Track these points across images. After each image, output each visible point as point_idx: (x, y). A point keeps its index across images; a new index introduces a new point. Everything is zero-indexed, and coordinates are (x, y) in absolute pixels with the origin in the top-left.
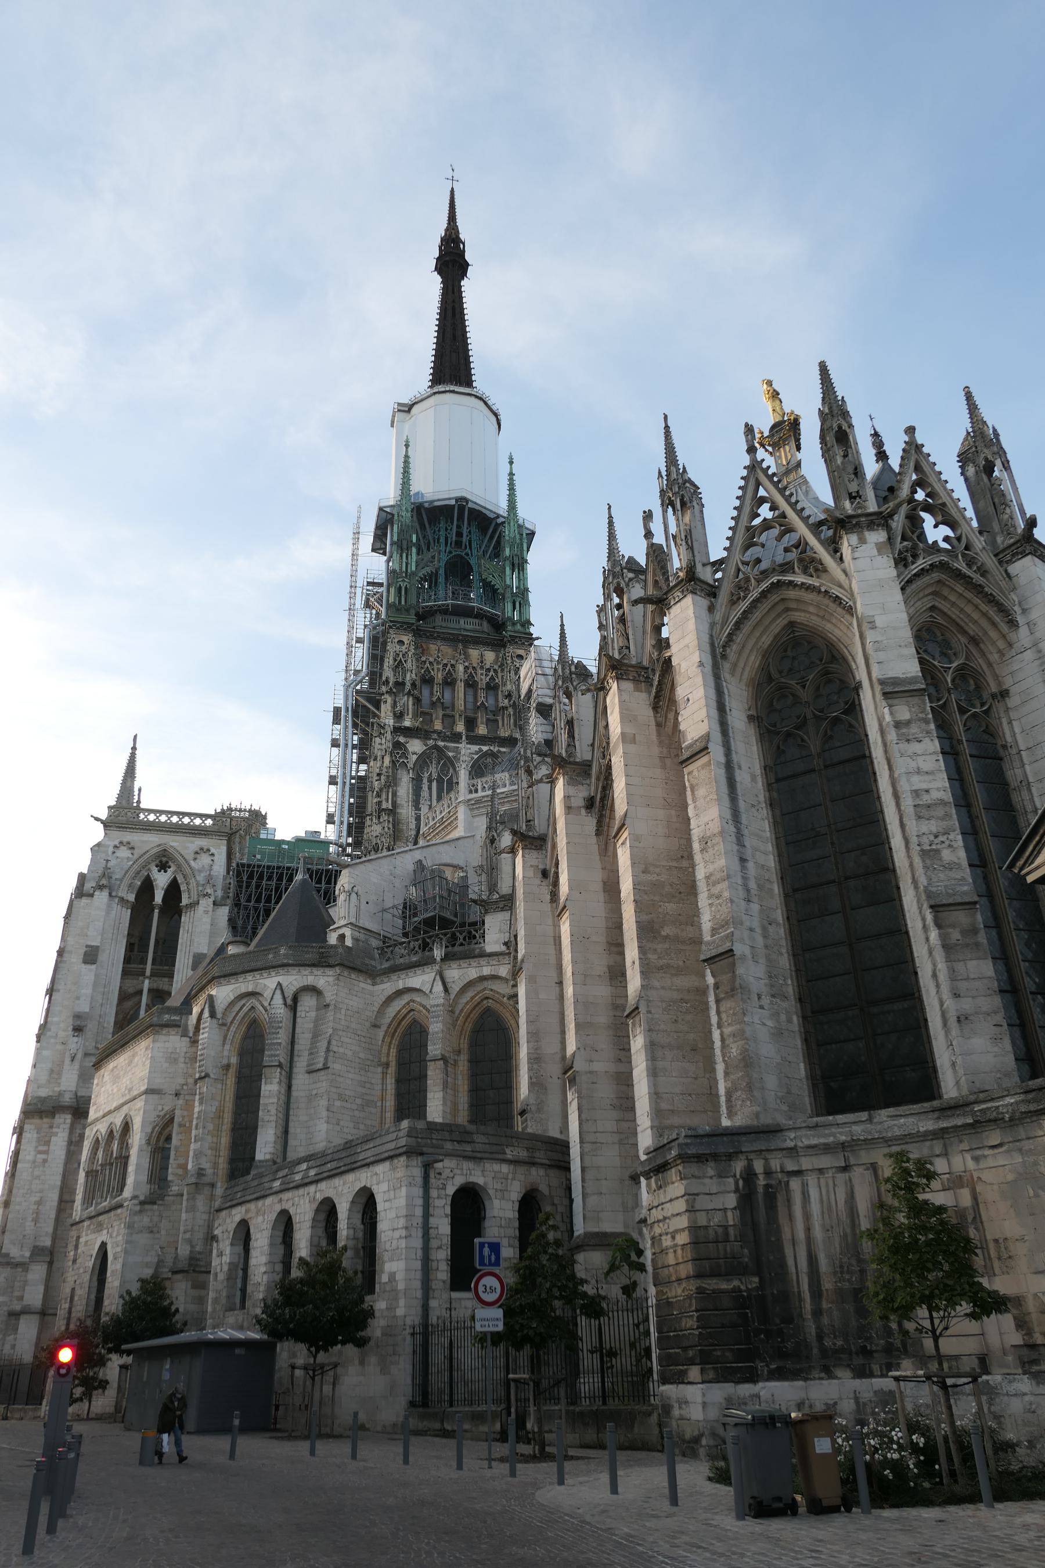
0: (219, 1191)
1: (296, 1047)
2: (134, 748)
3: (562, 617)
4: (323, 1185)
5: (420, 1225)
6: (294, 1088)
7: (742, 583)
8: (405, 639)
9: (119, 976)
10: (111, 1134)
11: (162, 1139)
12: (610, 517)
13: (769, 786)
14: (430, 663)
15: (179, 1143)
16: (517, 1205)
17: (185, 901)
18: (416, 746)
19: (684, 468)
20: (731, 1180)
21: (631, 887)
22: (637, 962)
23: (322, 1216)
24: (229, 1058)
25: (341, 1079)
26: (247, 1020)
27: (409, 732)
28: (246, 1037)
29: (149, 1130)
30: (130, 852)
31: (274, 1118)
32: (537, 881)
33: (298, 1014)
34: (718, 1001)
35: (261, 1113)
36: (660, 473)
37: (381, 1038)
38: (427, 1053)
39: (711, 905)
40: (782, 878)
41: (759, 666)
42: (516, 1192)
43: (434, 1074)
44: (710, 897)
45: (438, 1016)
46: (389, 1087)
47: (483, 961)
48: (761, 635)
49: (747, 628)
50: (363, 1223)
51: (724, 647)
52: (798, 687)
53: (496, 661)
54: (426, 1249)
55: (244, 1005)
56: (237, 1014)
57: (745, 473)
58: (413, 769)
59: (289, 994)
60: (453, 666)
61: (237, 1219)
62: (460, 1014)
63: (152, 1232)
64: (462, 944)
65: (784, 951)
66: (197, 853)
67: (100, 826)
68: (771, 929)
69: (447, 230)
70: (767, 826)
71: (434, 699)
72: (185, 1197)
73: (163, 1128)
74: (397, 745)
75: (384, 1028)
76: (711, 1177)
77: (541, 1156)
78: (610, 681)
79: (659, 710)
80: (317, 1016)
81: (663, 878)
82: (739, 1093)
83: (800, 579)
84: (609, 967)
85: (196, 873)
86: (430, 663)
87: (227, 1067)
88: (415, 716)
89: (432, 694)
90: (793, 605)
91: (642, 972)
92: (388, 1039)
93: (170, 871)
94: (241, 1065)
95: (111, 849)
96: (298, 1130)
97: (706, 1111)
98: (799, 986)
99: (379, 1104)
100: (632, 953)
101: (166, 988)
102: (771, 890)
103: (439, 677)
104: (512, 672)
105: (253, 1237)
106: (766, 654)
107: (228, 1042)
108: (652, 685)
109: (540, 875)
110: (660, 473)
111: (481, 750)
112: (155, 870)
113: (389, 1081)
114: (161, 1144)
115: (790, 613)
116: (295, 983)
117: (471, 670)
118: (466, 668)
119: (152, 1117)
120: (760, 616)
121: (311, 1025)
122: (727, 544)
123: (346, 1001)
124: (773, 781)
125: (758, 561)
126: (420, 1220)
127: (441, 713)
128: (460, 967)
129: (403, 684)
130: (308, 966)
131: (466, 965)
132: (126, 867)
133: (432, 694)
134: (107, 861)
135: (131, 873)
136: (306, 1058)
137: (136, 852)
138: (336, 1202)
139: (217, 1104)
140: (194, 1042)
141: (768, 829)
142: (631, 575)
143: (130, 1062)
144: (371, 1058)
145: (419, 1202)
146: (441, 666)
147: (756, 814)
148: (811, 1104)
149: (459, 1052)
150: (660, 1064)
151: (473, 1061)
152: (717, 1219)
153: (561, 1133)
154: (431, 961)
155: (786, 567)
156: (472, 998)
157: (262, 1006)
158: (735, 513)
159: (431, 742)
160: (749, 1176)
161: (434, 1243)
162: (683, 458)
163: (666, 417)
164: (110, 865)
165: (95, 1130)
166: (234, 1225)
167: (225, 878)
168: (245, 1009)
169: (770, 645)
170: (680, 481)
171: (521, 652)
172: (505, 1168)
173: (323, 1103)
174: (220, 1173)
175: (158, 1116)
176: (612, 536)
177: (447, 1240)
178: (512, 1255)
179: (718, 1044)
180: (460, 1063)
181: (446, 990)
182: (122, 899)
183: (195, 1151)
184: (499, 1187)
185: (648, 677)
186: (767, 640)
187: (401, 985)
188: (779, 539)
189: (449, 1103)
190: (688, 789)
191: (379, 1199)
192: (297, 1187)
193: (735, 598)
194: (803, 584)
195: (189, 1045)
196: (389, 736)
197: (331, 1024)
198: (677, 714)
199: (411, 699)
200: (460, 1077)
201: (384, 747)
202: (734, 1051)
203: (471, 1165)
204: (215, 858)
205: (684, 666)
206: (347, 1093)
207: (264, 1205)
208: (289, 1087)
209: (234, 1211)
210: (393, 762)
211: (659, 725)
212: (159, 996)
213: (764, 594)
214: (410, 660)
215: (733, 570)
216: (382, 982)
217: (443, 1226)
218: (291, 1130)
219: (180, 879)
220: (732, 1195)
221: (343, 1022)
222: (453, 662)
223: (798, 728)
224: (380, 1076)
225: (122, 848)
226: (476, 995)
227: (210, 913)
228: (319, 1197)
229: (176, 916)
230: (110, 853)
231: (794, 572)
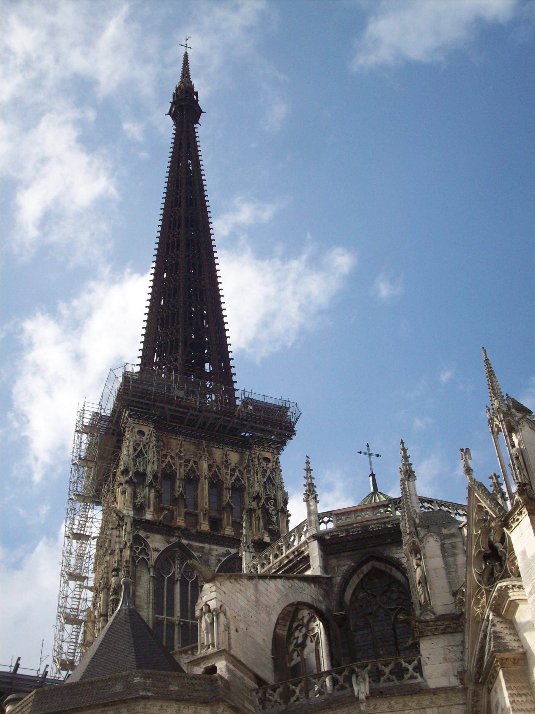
8: (145, 430)
14: (172, 457)
58: (154, 567)
64: (389, 680)
69: (181, 82)
71: (177, 494)
74: (137, 540)
88: (159, 510)
103: (182, 472)
104: (260, 474)
111: (228, 553)
117: (214, 468)
118: (210, 466)
127: (183, 511)
130: (177, 700)
131: (400, 706)
133: (173, 490)
159: (174, 540)
171: (268, 455)
196: (129, 527)
199: (152, 491)
210: (133, 558)
214: (150, 452)
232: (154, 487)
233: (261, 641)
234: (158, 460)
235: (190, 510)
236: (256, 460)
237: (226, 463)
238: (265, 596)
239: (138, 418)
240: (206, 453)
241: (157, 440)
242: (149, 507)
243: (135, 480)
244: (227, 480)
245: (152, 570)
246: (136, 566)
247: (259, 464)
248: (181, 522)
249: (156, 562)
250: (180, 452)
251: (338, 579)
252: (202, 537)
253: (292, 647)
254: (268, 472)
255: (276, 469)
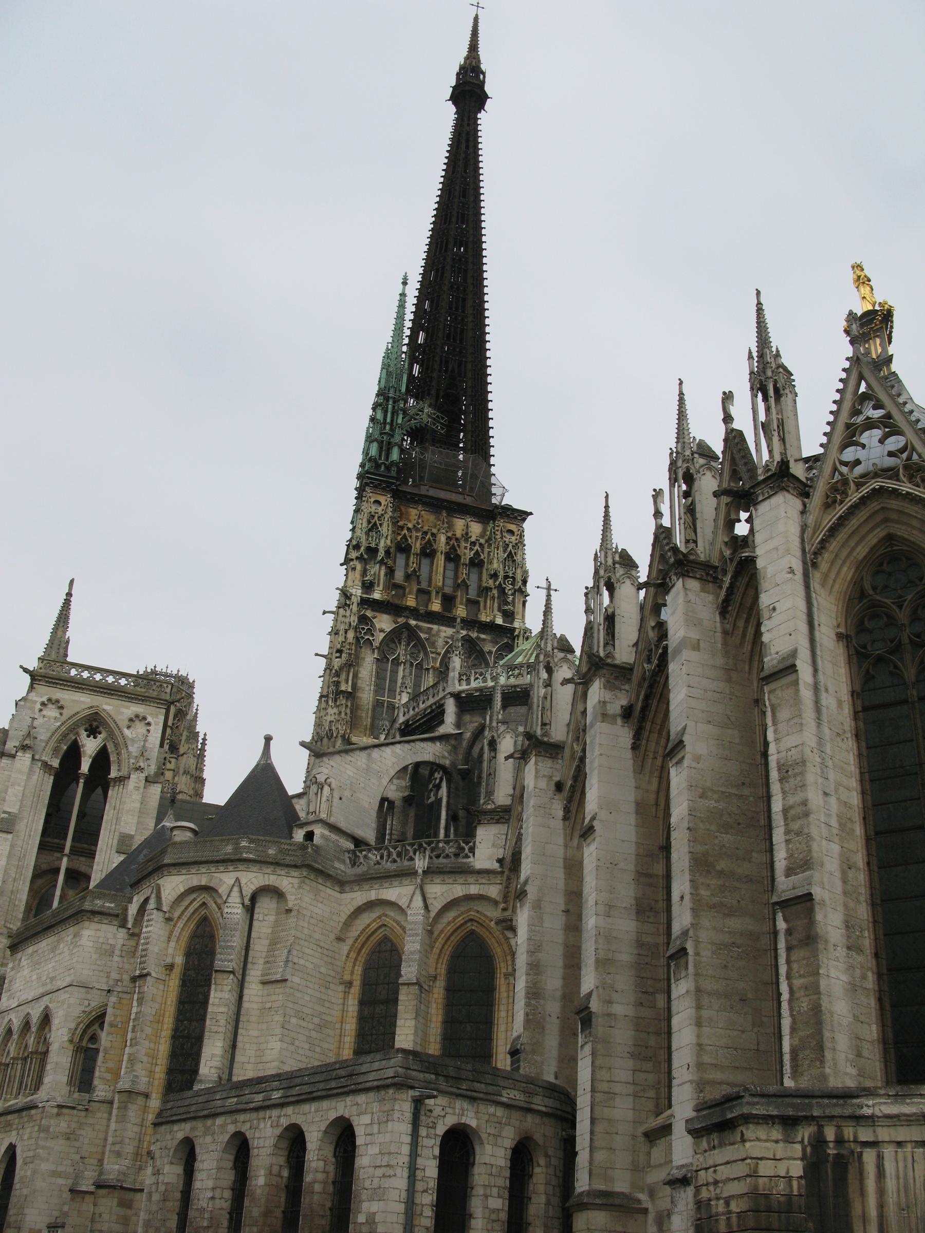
0: (155, 1103)
1: (251, 953)
2: (69, 594)
3: (607, 497)
4: (289, 1110)
5: (407, 1165)
6: (245, 998)
7: (839, 485)
8: (382, 499)
9: (36, 850)
10: (27, 1025)
11: (86, 1038)
12: (681, 394)
13: (856, 715)
15: (108, 1045)
16: (509, 1153)
17: (113, 774)
18: (384, 623)
19: (778, 351)
20: (798, 1147)
21: (686, 812)
22: (687, 898)
23: (284, 1144)
24: (173, 956)
25: (298, 994)
26: (196, 918)
27: (379, 606)
28: (194, 936)
29: (73, 1026)
30: (58, 711)
31: (222, 1029)
32: (550, 793)
33: (256, 916)
34: (789, 949)
35: (208, 1022)
36: (750, 352)
37: (345, 953)
38: (401, 976)
39: (788, 842)
40: (864, 818)
41: (852, 579)
42: (509, 1138)
43: (406, 1000)
44: (787, 832)
45: (417, 935)
46: (350, 1009)
47: (471, 879)
48: (857, 545)
49: (842, 535)
50: (335, 1156)
51: (815, 554)
52: (894, 607)
53: (482, 535)
54: (411, 1191)
55: (194, 900)
56: (186, 909)
57: (847, 365)
59: (248, 892)
60: (433, 535)
61: (180, 1136)
62: (439, 936)
63: (68, 1139)
65: (862, 898)
66: (131, 720)
67: (27, 679)
68: (851, 874)
69: (466, 58)
70: (852, 758)
72: (116, 1105)
73: (88, 1026)
74: (363, 619)
75: (350, 942)
76: (777, 1142)
77: (540, 1103)
78: (674, 577)
79: (728, 616)
80: (276, 921)
81: (721, 805)
82: (807, 1052)
83: (906, 487)
84: (636, 899)
85: (129, 743)
86: (409, 529)
87: (170, 967)
89: (407, 565)
90: (894, 516)
91: (693, 909)
92: (353, 955)
93: (100, 737)
94: (187, 967)
95: (38, 706)
96: (247, 1046)
97: (751, 1069)
98: (875, 939)
99: (338, 1026)
100: (681, 886)
101: (83, 869)
102: (853, 830)
103: (417, 546)
104: (501, 549)
105: (199, 1158)
106: (860, 566)
107: (174, 939)
108: (721, 587)
109: (553, 787)
110: (750, 352)
112: (84, 734)
113: (350, 1002)
114: (84, 1044)
115: (889, 524)
116: (254, 881)
117: (453, 542)
118: (449, 538)
119: (77, 1011)
120: (858, 523)
121: (269, 931)
122: (824, 440)
123: (311, 907)
124: (860, 709)
125: (858, 462)
126: (406, 1159)
127: (415, 588)
128: (443, 883)
129: (376, 550)
130: (272, 863)
131: (451, 881)
132: (53, 728)
133: (407, 565)
134: (34, 719)
135: (57, 736)
136: (261, 967)
137: (64, 712)
138: (304, 1130)
139: (157, 1006)
140: (134, 935)
141: (852, 762)
142: (702, 461)
143: (54, 950)
144: (333, 973)
145: (408, 1139)
146: (419, 534)
147: (841, 744)
148: (881, 1070)
149: (435, 977)
150: (705, 1013)
151: (450, 990)
152: (782, 1186)
153: (556, 1078)
154: (413, 873)
155: (890, 473)
156: (455, 918)
157: (215, 903)
158: (834, 408)
159: (401, 620)
160: (819, 1142)
161: (420, 1186)
162: (776, 341)
163: (758, 293)
164: (36, 723)
165: (6, 1020)
166: (176, 1142)
167: (159, 752)
168: (196, 905)
169: (865, 557)
170: (774, 366)
172: (500, 1112)
173: (278, 1018)
174: (156, 1083)
175: (84, 1012)
176: (682, 415)
177: (433, 1184)
178: (500, 1207)
179: (785, 996)
180: (436, 990)
181: (426, 907)
182: (46, 765)
183: (130, 1055)
184: (491, 1130)
185: (716, 578)
186: (862, 551)
187: (373, 895)
188: (882, 441)
189: (420, 1033)
190: (769, 709)
191: (359, 1131)
192: (256, 1109)
193: (829, 500)
194: (908, 493)
195: (126, 937)
196: (355, 608)
197: (293, 932)
198: (759, 625)
199: (383, 568)
200: (434, 1006)
201: (347, 620)
202: (804, 1005)
203: (465, 1105)
204: (152, 728)
205: (770, 571)
206: (305, 1010)
207: (214, 1124)
208: (241, 997)
209: (176, 1127)
210: (357, 639)
211: (725, 632)
212: (77, 878)
213: (863, 500)
214: (385, 524)
215: (828, 469)
216: (352, 891)
217: (430, 1168)
218: (239, 1045)
219: (111, 747)
220: (799, 1162)
221: (306, 931)
222: (434, 531)
223: (892, 652)
224: (341, 995)
225: (50, 706)
226: (460, 915)
227: (141, 790)
228: (284, 1122)
229: (99, 790)
230: (37, 710)
231: (898, 480)
232: (386, 564)
233: (366, 805)
234: (394, 532)
235: (424, 585)
236: (498, 533)
237: (466, 536)
238: (379, 763)
239: (375, 487)
240: (446, 525)
241: (394, 511)
242: (378, 585)
243: (366, 556)
244: (465, 554)
245: (376, 651)
246: (361, 647)
247: (502, 538)
248: (411, 602)
249: (381, 644)
250: (418, 523)
251: (468, 735)
252: (431, 617)
253: (431, 786)
254: (510, 547)
255: (520, 544)
